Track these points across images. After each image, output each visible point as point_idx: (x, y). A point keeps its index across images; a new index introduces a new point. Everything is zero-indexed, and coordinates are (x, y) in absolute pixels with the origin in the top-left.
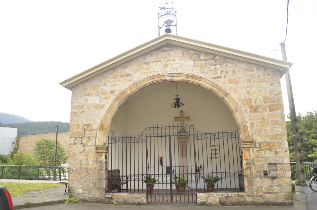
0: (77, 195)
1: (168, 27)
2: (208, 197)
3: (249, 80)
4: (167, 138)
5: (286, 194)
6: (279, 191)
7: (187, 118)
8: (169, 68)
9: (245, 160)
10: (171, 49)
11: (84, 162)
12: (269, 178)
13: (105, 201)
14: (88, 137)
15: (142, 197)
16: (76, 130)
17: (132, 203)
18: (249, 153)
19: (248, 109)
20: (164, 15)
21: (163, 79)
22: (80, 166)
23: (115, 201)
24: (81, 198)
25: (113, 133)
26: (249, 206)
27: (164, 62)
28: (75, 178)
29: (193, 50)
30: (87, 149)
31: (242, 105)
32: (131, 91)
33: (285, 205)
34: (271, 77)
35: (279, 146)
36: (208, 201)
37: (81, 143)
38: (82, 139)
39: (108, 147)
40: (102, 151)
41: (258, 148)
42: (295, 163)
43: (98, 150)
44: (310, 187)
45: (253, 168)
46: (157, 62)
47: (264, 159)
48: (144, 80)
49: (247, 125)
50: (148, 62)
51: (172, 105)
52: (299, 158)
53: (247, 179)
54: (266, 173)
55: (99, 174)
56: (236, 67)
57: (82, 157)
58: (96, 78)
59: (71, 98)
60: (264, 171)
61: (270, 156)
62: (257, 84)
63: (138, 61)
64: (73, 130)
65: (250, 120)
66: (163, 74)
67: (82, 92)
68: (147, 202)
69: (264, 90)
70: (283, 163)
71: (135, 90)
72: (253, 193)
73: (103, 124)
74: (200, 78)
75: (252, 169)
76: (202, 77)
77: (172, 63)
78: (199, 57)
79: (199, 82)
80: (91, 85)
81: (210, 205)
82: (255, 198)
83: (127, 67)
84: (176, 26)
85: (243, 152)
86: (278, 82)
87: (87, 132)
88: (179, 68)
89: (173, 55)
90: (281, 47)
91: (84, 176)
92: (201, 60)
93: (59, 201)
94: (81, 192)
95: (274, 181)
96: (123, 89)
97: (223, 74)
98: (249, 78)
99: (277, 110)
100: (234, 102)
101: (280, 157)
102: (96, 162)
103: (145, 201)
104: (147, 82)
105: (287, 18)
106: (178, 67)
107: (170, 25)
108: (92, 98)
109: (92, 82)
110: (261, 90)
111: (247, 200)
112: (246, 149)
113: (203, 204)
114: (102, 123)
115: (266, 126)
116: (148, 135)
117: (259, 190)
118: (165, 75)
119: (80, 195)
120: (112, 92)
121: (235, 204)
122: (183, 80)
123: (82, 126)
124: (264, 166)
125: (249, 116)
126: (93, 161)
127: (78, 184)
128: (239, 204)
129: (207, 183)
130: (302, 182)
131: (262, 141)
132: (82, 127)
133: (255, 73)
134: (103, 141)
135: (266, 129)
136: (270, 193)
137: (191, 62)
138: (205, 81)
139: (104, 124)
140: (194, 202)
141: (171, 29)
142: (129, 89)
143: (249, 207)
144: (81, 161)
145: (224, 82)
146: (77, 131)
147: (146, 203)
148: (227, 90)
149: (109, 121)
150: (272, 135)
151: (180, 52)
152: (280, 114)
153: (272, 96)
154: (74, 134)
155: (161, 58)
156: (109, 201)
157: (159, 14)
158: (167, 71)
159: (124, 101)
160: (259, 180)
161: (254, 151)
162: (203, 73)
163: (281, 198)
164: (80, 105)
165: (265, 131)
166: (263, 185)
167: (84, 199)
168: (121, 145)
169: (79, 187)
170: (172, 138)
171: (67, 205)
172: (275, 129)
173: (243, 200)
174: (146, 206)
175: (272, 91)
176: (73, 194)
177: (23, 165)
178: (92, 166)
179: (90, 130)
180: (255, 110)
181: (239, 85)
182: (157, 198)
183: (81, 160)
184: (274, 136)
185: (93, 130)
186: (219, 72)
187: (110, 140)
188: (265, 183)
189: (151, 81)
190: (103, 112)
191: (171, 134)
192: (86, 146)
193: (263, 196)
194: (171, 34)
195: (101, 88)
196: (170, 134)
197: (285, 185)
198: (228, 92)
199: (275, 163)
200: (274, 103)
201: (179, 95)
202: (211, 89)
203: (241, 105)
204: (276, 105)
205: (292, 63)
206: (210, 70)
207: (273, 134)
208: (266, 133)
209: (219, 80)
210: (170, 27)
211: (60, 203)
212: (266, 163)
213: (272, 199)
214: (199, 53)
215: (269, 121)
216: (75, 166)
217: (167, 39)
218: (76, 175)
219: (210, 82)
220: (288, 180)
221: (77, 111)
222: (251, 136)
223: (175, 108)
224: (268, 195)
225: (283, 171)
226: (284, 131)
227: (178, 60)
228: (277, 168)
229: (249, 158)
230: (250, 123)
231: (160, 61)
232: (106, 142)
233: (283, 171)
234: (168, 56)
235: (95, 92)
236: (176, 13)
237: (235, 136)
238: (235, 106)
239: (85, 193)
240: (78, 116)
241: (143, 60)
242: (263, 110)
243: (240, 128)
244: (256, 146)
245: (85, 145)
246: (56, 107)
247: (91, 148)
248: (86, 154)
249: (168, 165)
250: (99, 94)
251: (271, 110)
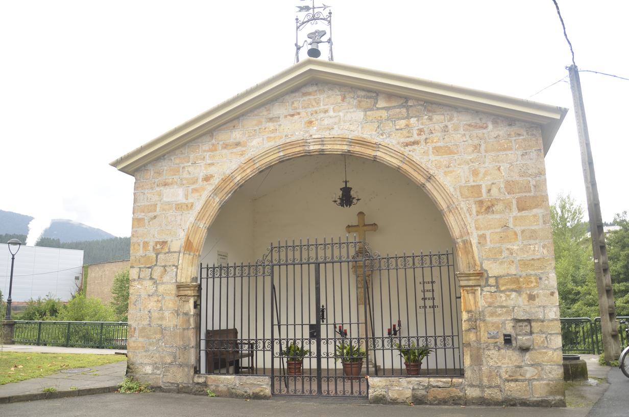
0: (143, 376)
1: (314, 46)
2: (389, 387)
3: (477, 148)
4: (312, 267)
5: (551, 382)
6: (536, 377)
7: (370, 228)
8: (315, 128)
9: (466, 312)
10: (319, 90)
11: (155, 315)
12: (514, 350)
13: (193, 390)
14: (162, 266)
15: (261, 383)
16: (141, 252)
17: (243, 395)
18: (475, 298)
19: (474, 206)
20: (308, 21)
21: (303, 150)
22: (148, 323)
23: (212, 390)
24: (150, 384)
25: (224, 257)
26: (473, 407)
27: (306, 115)
28: (140, 345)
29: (363, 89)
30: (161, 288)
31: (462, 198)
32: (244, 174)
33: (547, 406)
34: (523, 139)
35: (537, 282)
36: (390, 395)
37: (151, 278)
38: (152, 270)
39: (200, 287)
40: (189, 293)
41: (492, 287)
42: (600, 319)
43: (181, 292)
44: (621, 369)
45: (483, 329)
46: (292, 115)
47: (504, 310)
48: (267, 153)
49: (471, 239)
50: (276, 118)
51: (335, 201)
52: (607, 308)
53: (469, 352)
54: (508, 340)
55: (183, 337)
56: (449, 121)
57: (152, 304)
58: (178, 152)
59: (132, 191)
60: (505, 335)
61: (519, 304)
62: (493, 154)
63: (257, 116)
64: (137, 253)
65: (477, 229)
66: (304, 141)
67: (152, 179)
68: (272, 394)
69: (508, 166)
70: (545, 318)
71: (250, 174)
72: (481, 380)
73: (190, 241)
74: (377, 146)
75: (480, 331)
76: (380, 144)
77: (321, 118)
78: (376, 103)
79: (375, 155)
80: (169, 165)
81: (394, 402)
82: (485, 391)
83: (236, 127)
84: (329, 43)
85: (462, 295)
86: (538, 149)
87: (161, 256)
88: (335, 126)
89: (323, 101)
90: (570, 74)
91: (154, 340)
92: (378, 109)
93: (109, 388)
94: (150, 372)
95: (525, 355)
96: (228, 172)
97: (424, 137)
98: (476, 142)
99: (534, 208)
100: (445, 192)
101: (540, 306)
102: (178, 315)
103: (268, 391)
104: (273, 157)
105: (559, 13)
106: (335, 124)
107: (318, 41)
108: (172, 190)
109: (172, 160)
110: (502, 167)
111: (468, 394)
112: (468, 288)
113: (380, 400)
114: (190, 238)
115: (510, 242)
116: (275, 262)
117: (494, 373)
118: (308, 141)
119: (148, 377)
120: (207, 179)
121: (444, 402)
122: (344, 151)
123: (152, 244)
124: (505, 324)
125: (476, 221)
126: (172, 313)
127: (145, 356)
128: (452, 402)
129: (406, 356)
130: (614, 358)
131: (501, 274)
132: (152, 248)
133: (489, 132)
134: (191, 274)
135: (511, 247)
136: (517, 380)
137: (360, 115)
138: (387, 151)
139: (192, 241)
140: (364, 395)
141: (319, 49)
142: (240, 170)
143: (470, 408)
144: (149, 312)
145: (424, 152)
146: (144, 254)
147: (270, 393)
148: (432, 170)
149: (202, 233)
150: (523, 260)
151: (338, 95)
152: (541, 215)
153: (524, 178)
154: (137, 261)
155: (301, 107)
156: (200, 391)
157: (297, 19)
158: (311, 134)
159: (230, 195)
160: (493, 352)
161: (485, 293)
162: (382, 135)
163: (539, 392)
164: (149, 205)
165: (508, 252)
166: (503, 363)
167: (155, 386)
168: (238, 280)
169: (145, 361)
170: (322, 266)
171: (121, 396)
172: (530, 248)
173: (461, 394)
174: (269, 401)
175: (524, 168)
176: (135, 375)
177: (84, 320)
178: (171, 321)
179: (167, 253)
180: (489, 209)
181: (456, 157)
182: (307, 387)
183: (151, 309)
184: (527, 263)
185: (172, 252)
186: (415, 132)
187: (204, 271)
188: (506, 360)
189: (281, 154)
190: (190, 218)
191: (320, 260)
192: (159, 283)
193: (502, 386)
194: (320, 59)
195: (188, 171)
196: (317, 258)
197: (549, 364)
198: (431, 172)
199: (528, 318)
200: (528, 194)
201: (350, 180)
202: (399, 168)
203: (460, 198)
204: (533, 197)
205: (565, 109)
206: (397, 130)
207: (524, 258)
208: (511, 256)
209: (414, 149)
210: (319, 44)
211: (109, 392)
212: (509, 318)
213: (520, 393)
214: (374, 95)
215: (517, 232)
216: (140, 322)
217: (311, 70)
218: (141, 339)
219: (396, 153)
220: (555, 353)
221: (143, 217)
222: (479, 263)
223: (342, 206)
224: (512, 384)
225: (544, 336)
226: (548, 251)
227: (334, 111)
228: (532, 329)
229: (473, 308)
230: (478, 235)
231: (299, 114)
232: (195, 275)
233: (544, 336)
234: (314, 103)
235: (176, 178)
236: (330, 16)
237: (448, 262)
238: (447, 202)
239: (156, 374)
240: (145, 226)
241: (265, 113)
242: (505, 208)
243: (457, 245)
244: (489, 283)
245: (158, 282)
246: (112, 210)
247: (168, 287)
248: (160, 298)
249: (314, 322)
250: (184, 182)
251: (521, 209)
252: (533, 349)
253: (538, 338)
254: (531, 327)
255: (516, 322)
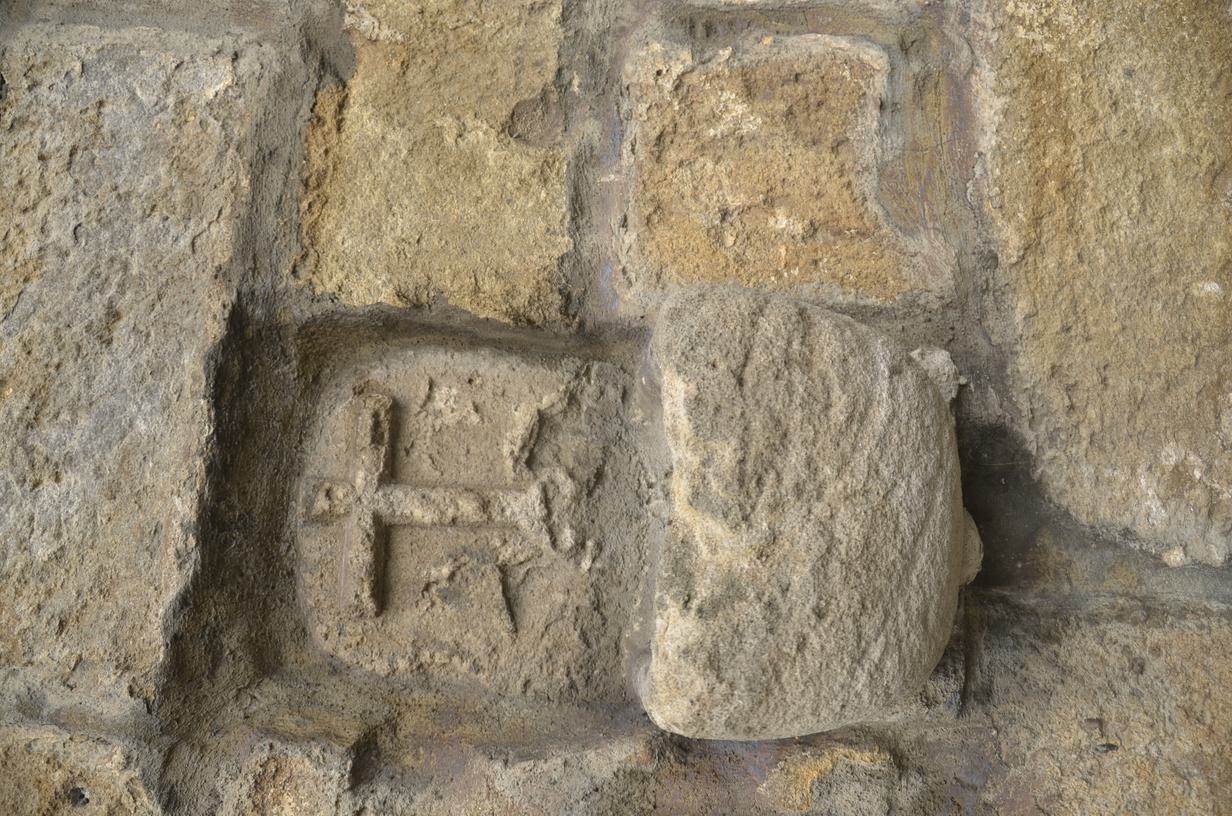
199: (191, 369)
252: (960, 318)
253: (721, 184)
254: (408, 324)
255: (266, 662)
